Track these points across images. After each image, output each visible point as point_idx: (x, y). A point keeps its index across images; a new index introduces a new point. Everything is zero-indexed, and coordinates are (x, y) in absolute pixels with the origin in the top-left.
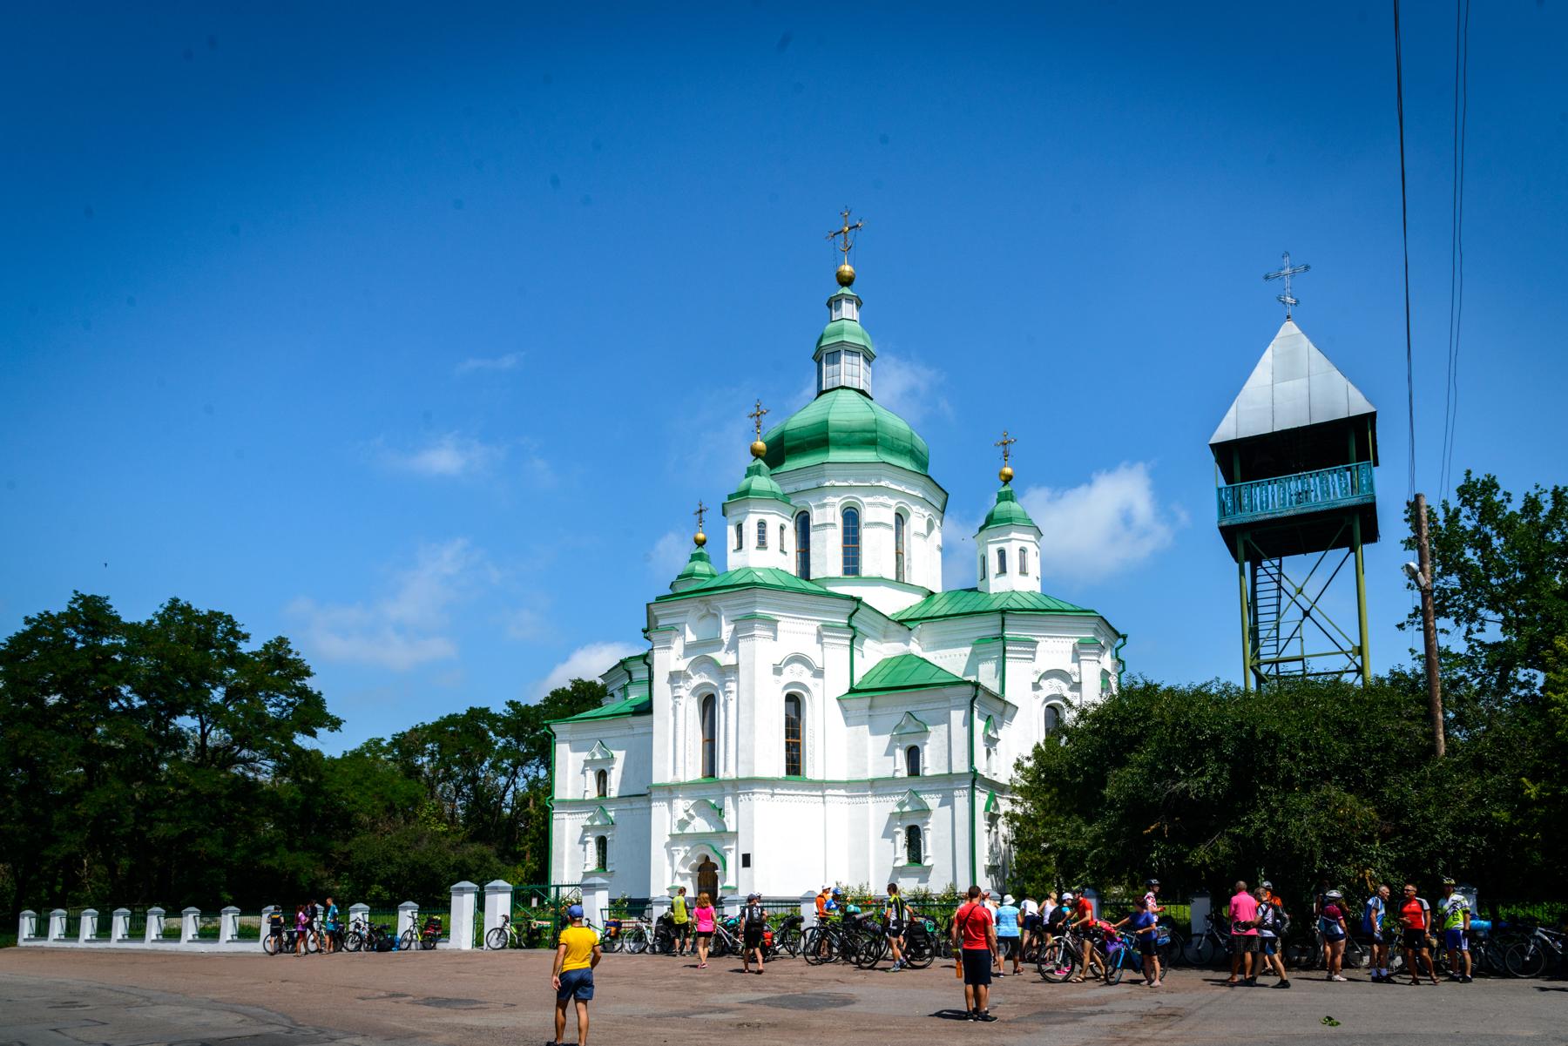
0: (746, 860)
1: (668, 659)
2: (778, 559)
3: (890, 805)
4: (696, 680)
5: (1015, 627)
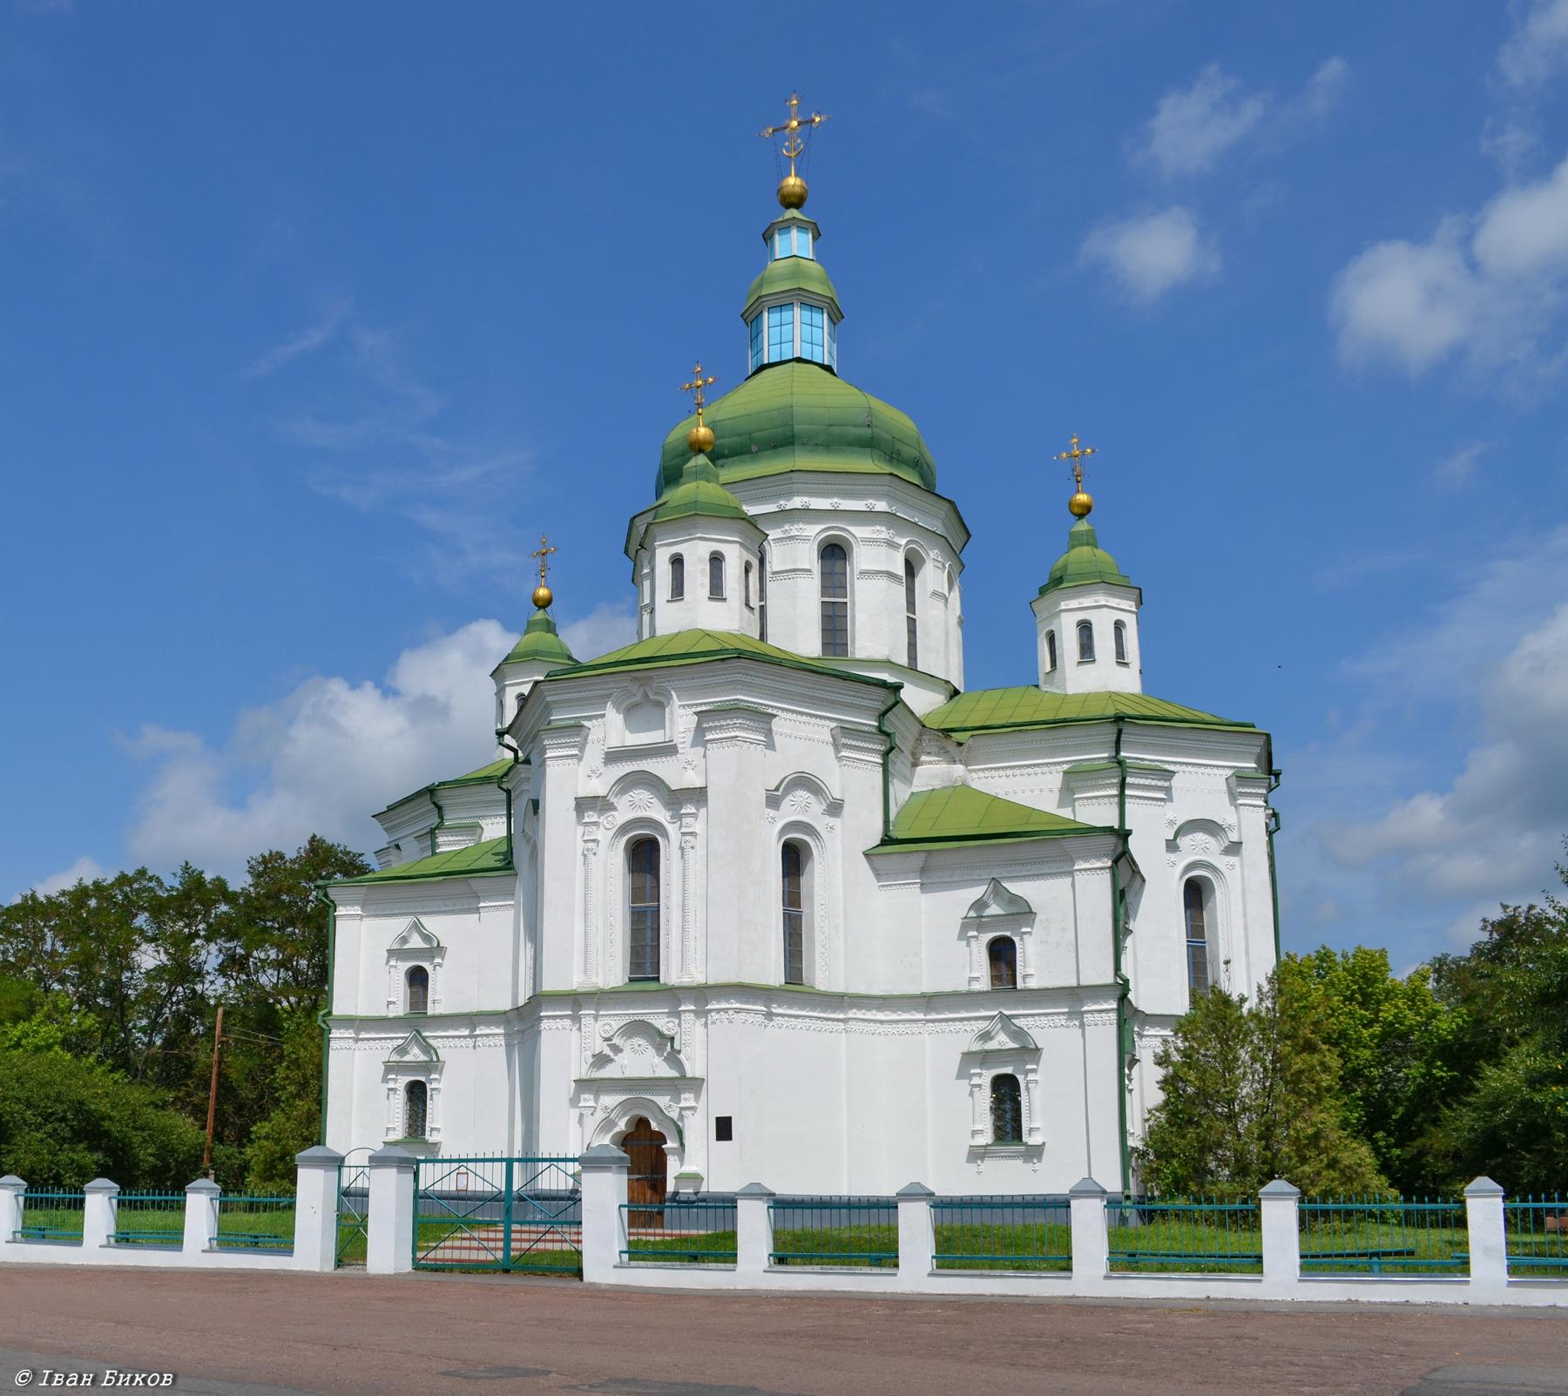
0: (724, 1129)
1: (568, 776)
2: (724, 619)
3: (961, 1034)
4: (623, 814)
5: (1134, 746)
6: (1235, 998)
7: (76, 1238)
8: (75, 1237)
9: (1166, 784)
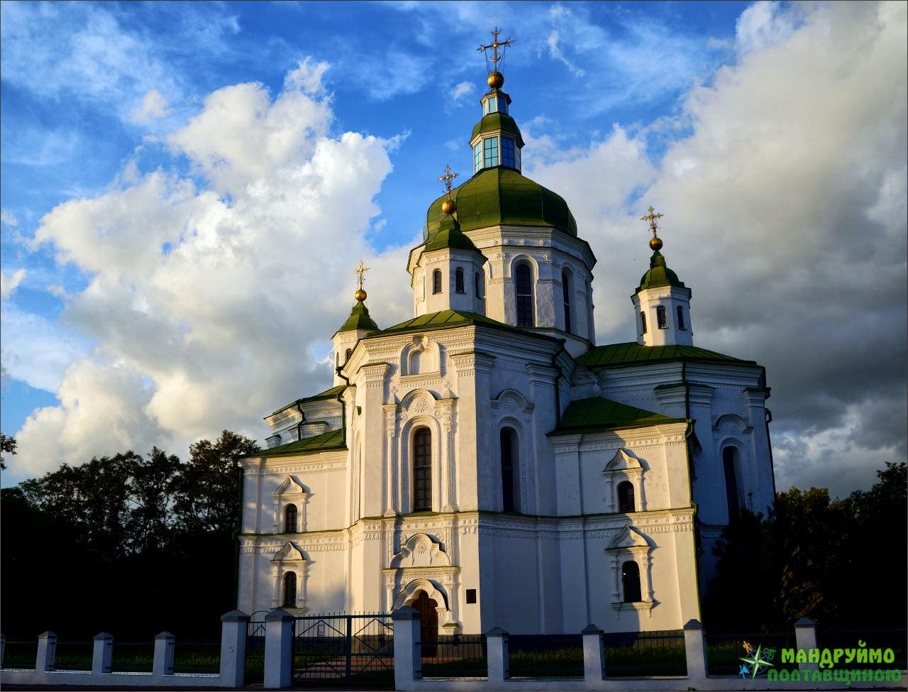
6: (756, 514)
7: (31, 665)
8: (31, 665)
9: (711, 395)
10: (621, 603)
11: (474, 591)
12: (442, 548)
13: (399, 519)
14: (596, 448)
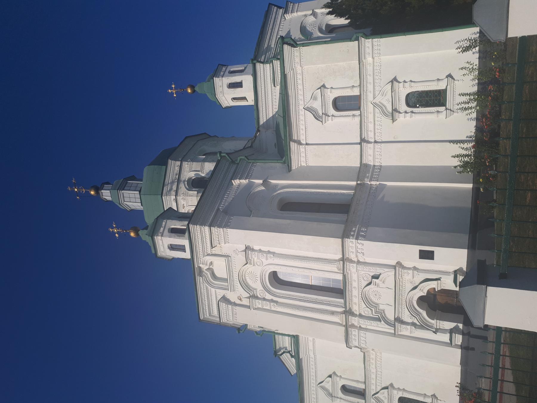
10: (446, 109)
11: (421, 252)
12: (376, 277)
13: (348, 313)
14: (302, 130)
